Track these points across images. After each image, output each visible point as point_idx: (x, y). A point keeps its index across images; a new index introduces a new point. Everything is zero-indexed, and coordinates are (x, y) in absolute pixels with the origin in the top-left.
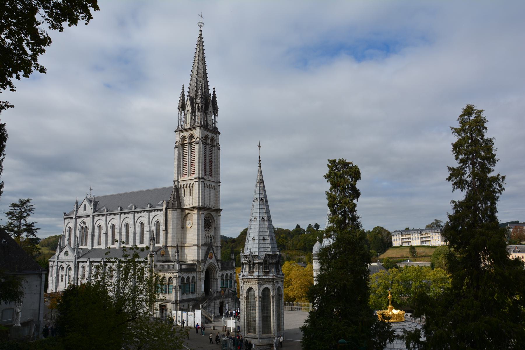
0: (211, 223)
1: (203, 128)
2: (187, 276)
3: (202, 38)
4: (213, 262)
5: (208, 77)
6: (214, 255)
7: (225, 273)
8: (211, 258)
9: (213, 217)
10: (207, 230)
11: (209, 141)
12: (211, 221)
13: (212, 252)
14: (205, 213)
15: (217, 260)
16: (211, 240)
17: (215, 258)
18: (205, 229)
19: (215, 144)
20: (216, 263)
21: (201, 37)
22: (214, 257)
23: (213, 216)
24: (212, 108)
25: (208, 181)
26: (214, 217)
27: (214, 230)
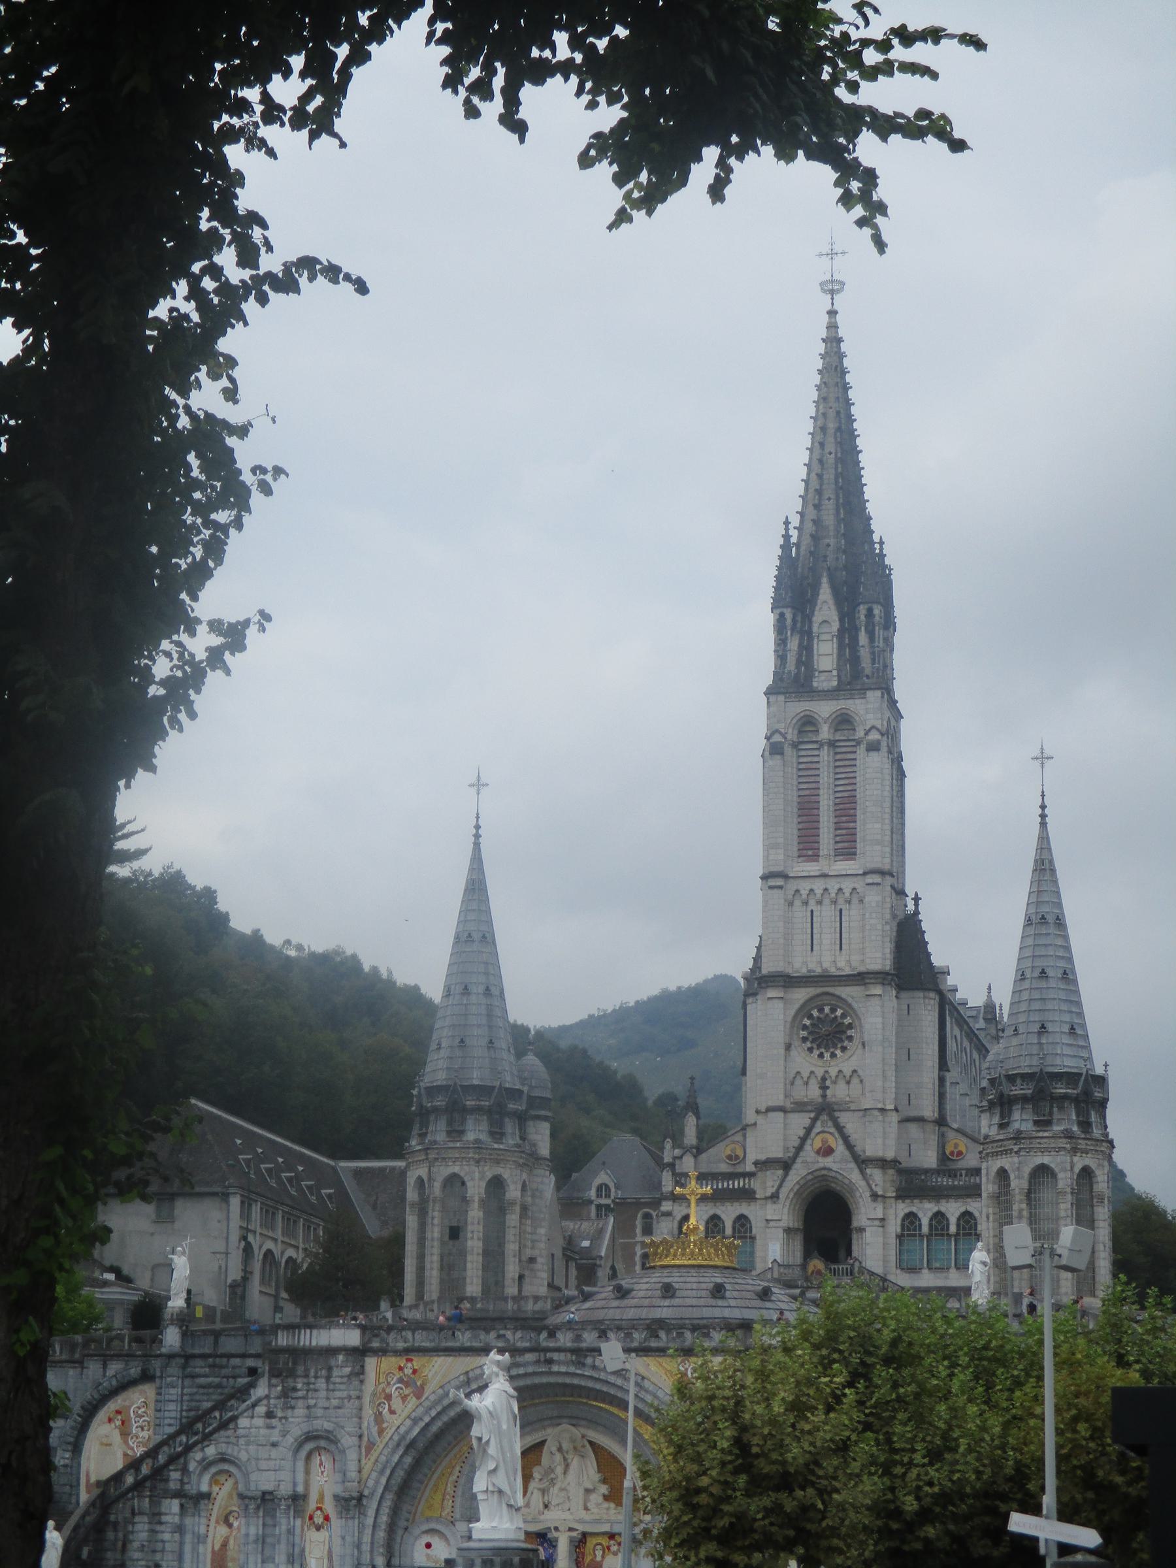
0: (850, 1026)
1: (781, 698)
2: (711, 1212)
3: (840, 340)
4: (835, 1167)
6: (840, 1141)
7: (925, 1210)
8: (828, 1151)
9: (850, 1006)
10: (827, 1055)
11: (825, 733)
12: (847, 1021)
13: (833, 1130)
14: (801, 995)
15: (862, 1163)
16: (824, 1088)
17: (847, 1153)
18: (816, 1052)
19: (860, 733)
20: (856, 1172)
21: (833, 341)
22: (840, 1148)
23: (850, 1000)
24: (833, 607)
25: (817, 880)
26: (855, 1005)
27: (860, 1051)
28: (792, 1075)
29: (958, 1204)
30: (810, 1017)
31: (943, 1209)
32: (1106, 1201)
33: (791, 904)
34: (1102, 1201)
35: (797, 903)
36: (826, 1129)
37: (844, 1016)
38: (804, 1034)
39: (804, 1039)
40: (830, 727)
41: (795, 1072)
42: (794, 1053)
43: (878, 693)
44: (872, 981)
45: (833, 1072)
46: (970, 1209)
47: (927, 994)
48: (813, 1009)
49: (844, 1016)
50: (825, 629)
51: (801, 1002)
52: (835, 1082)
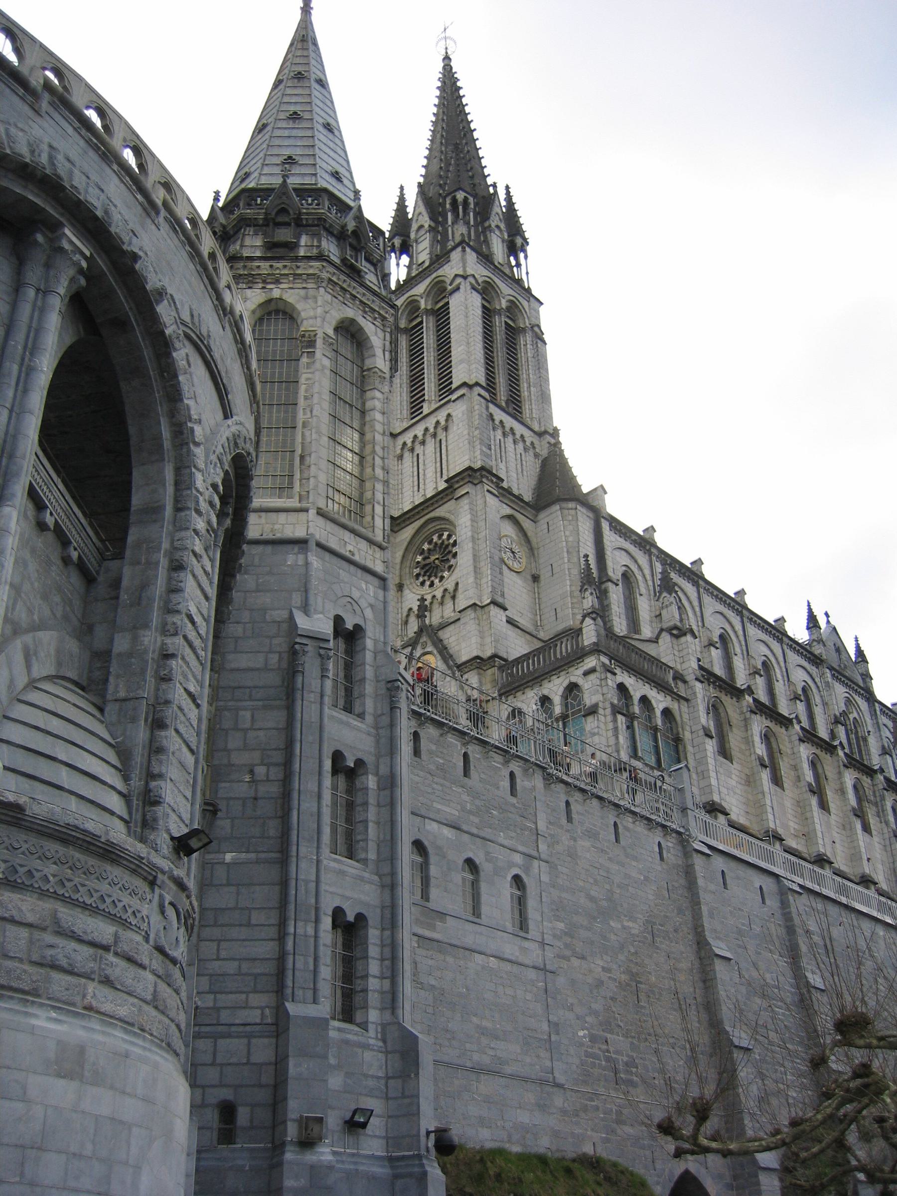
5: (475, 130)
12: (451, 541)
28: (405, 614)
29: (561, 679)
30: (422, 552)
31: (546, 692)
32: (319, 343)
33: (400, 457)
34: (312, 343)
35: (407, 455)
36: (426, 650)
37: (449, 536)
38: (417, 571)
39: (418, 576)
40: (426, 301)
41: (406, 610)
42: (406, 592)
43: (460, 249)
44: (461, 483)
45: (439, 594)
46: (574, 679)
47: (564, 505)
48: (423, 543)
49: (449, 536)
50: (422, 232)
51: (408, 540)
52: (442, 603)
